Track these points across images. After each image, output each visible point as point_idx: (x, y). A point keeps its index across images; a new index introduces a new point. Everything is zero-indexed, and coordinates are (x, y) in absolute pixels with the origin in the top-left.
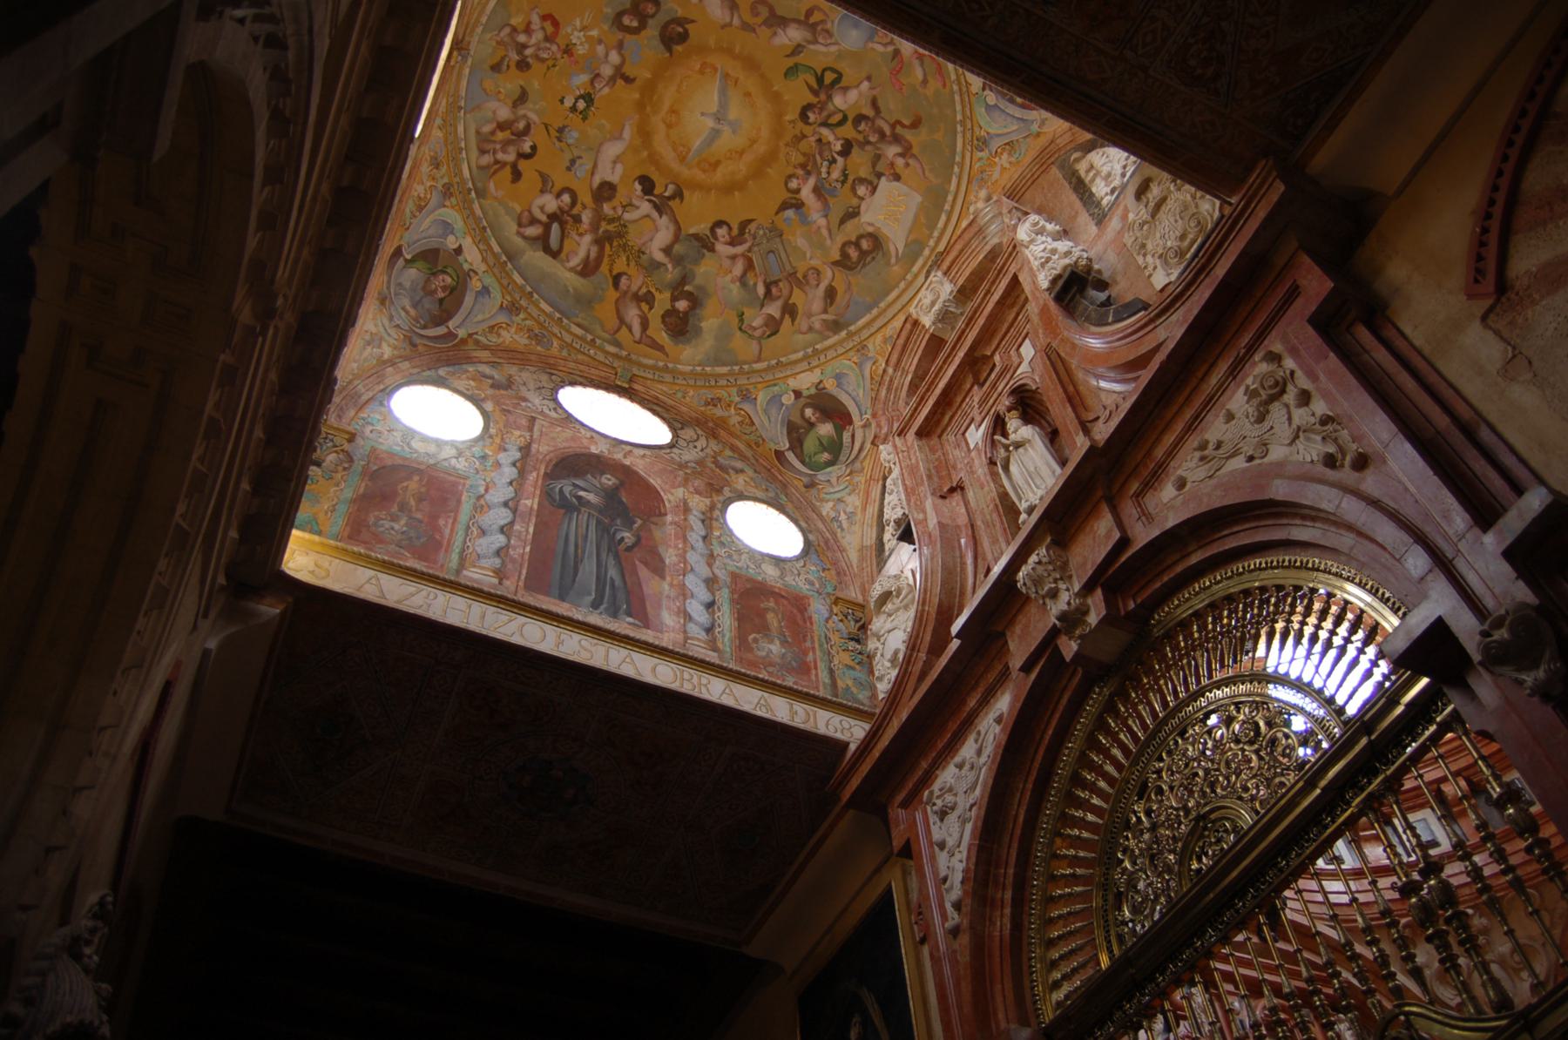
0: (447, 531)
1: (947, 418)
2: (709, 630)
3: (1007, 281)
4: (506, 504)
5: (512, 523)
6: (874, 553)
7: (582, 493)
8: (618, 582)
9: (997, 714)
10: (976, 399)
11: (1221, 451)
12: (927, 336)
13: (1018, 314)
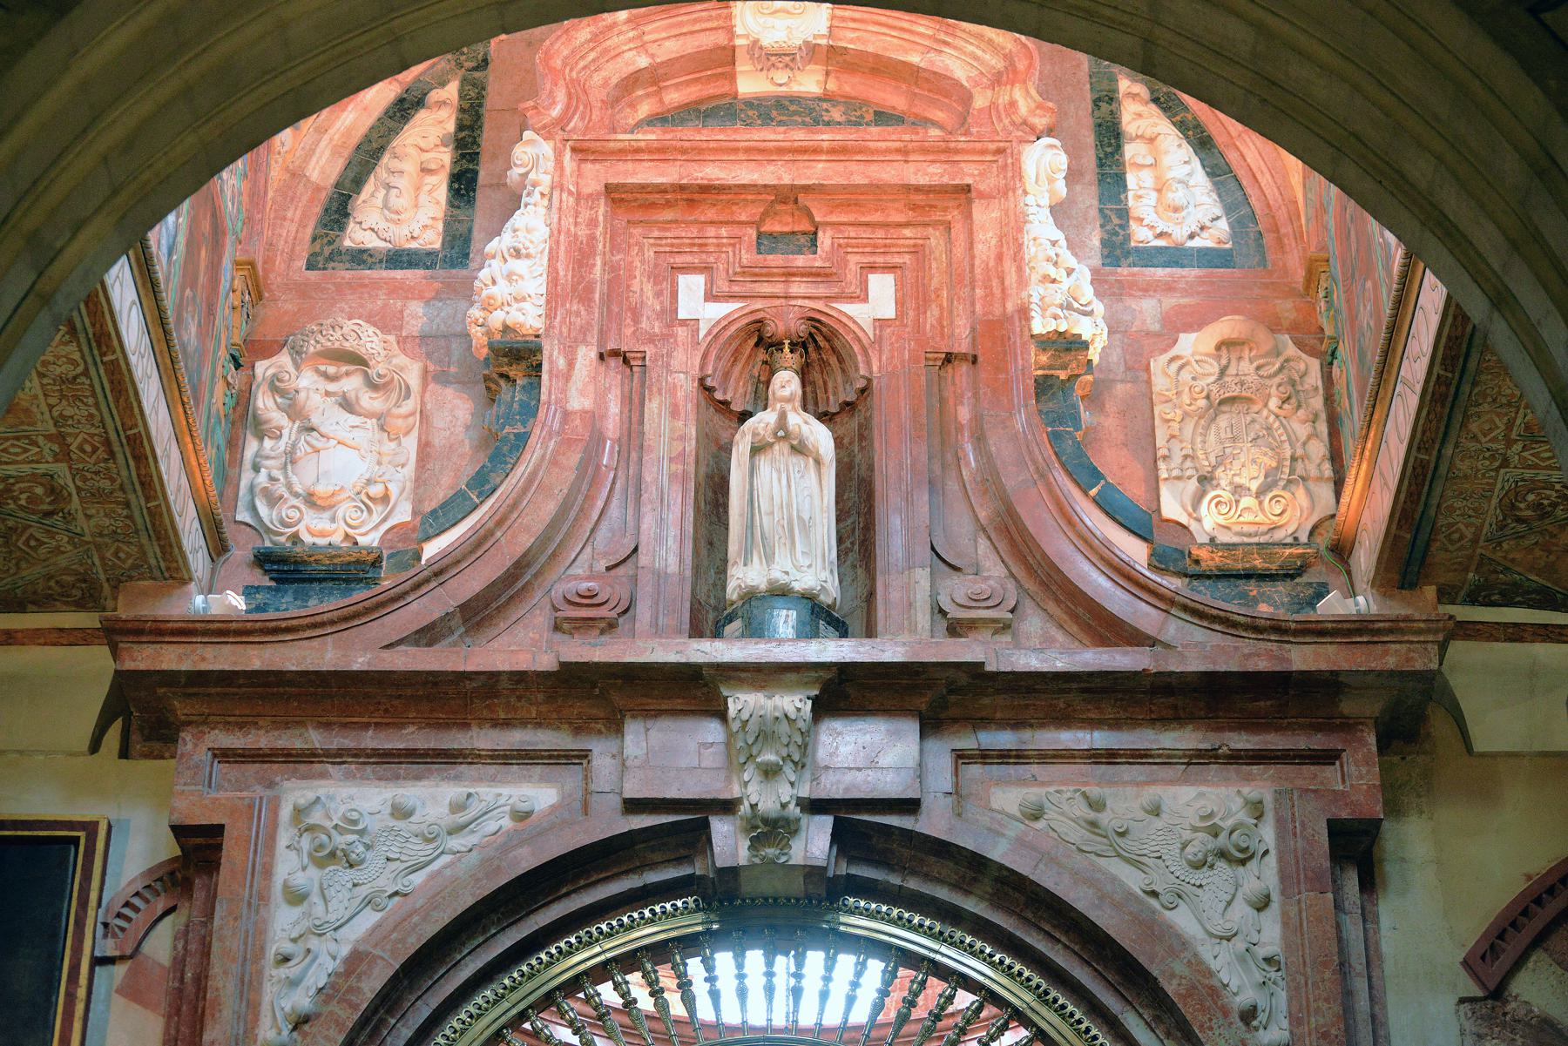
1: (668, 215)
3: (945, 180)
6: (318, 210)
9: (525, 807)
10: (747, 257)
11: (1119, 840)
12: (721, 38)
13: (907, 225)
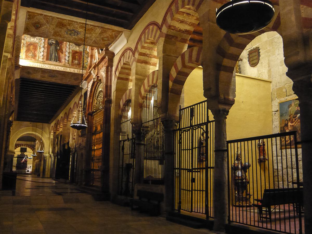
0: (36, 54)
2: (68, 61)
4: (43, 47)
5: (44, 50)
7: (53, 42)
8: (57, 56)
